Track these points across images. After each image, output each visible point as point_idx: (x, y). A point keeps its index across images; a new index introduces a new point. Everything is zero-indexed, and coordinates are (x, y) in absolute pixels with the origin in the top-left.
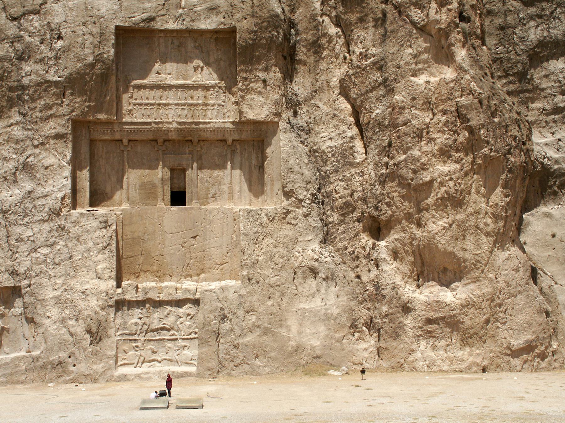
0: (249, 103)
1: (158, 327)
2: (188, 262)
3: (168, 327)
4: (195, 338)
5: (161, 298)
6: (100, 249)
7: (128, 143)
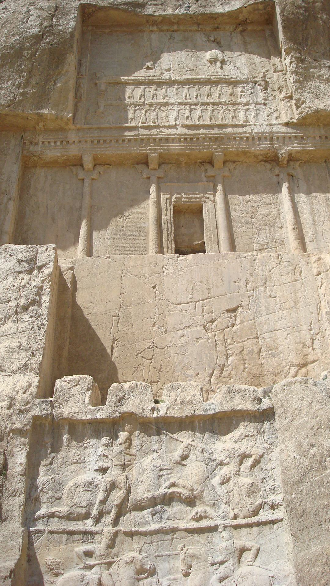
0: (313, 90)
1: (157, 494)
2: (222, 361)
3: (185, 493)
4: (273, 522)
5: (162, 413)
6: (12, 311)
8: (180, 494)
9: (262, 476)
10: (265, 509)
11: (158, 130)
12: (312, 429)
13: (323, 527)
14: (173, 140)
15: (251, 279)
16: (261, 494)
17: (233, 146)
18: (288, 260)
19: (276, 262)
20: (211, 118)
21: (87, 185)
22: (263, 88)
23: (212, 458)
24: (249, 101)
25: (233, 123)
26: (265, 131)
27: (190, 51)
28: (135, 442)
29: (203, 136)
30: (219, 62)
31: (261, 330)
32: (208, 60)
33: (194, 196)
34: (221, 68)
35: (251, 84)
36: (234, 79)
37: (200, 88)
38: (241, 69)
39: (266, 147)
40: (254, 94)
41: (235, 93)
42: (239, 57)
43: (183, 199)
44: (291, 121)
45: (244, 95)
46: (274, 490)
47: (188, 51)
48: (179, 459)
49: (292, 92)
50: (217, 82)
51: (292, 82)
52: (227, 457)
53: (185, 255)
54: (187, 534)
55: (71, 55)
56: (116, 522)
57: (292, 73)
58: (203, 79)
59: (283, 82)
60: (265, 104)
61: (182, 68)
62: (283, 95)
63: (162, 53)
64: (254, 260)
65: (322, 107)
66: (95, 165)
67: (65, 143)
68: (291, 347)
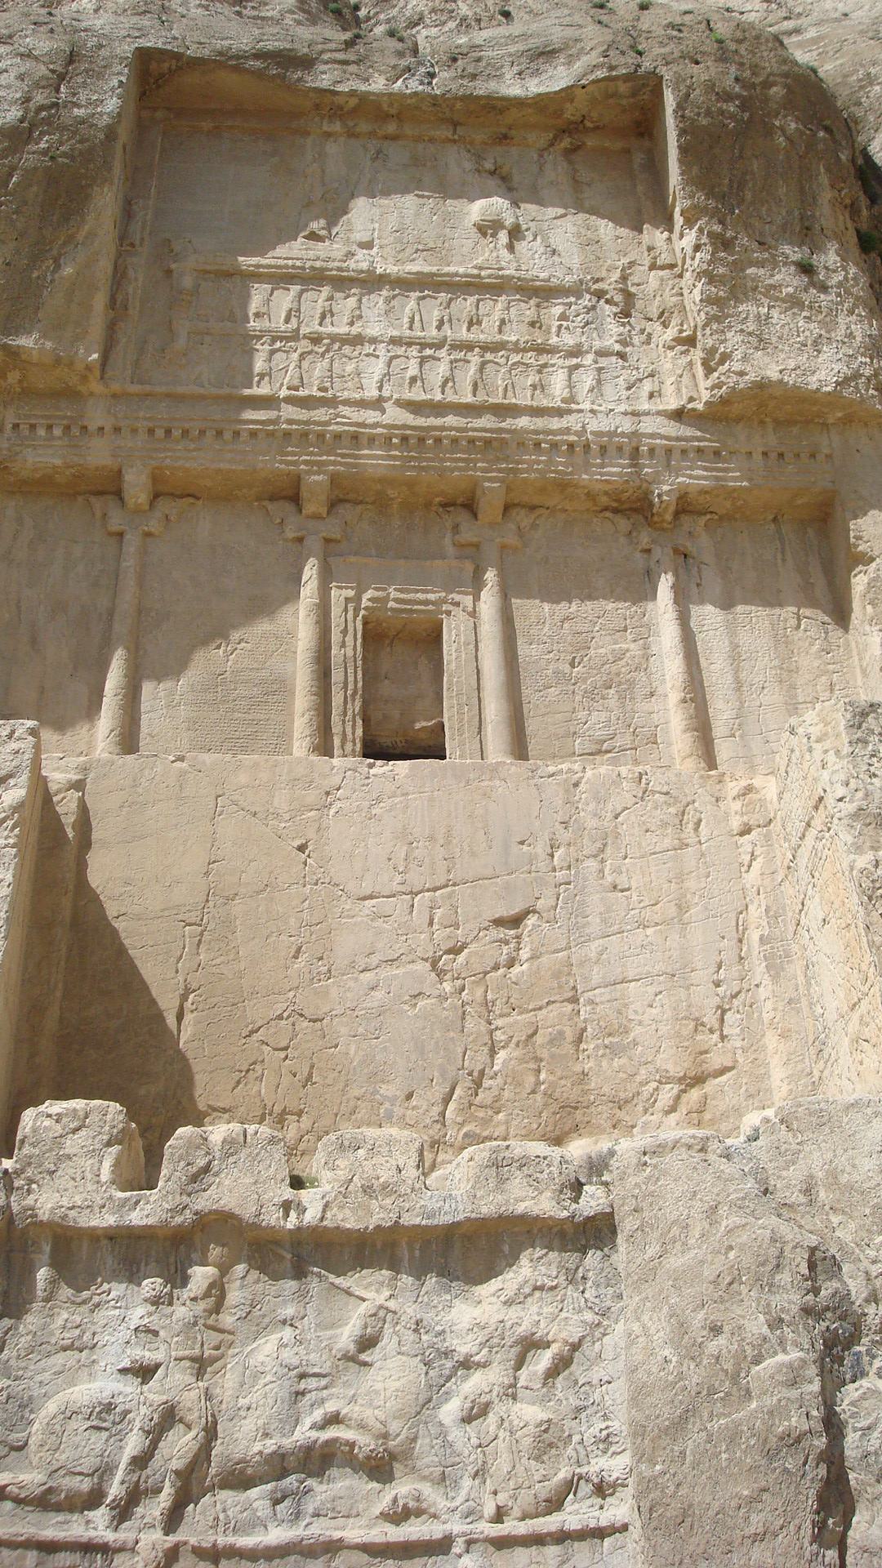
1: (287, 1443)
2: (477, 1059)
3: (365, 1443)
4: (600, 1533)
5: (311, 1216)
7: (152, 504)
8: (352, 1445)
9: (574, 1402)
10: (580, 1494)
11: (332, 411)
12: (715, 1283)
13: (735, 1557)
14: (372, 440)
15: (564, 836)
16: (570, 1451)
17: (531, 467)
18: (665, 789)
19: (634, 793)
20: (475, 386)
21: (132, 549)
22: (618, 310)
23: (443, 1347)
24: (580, 345)
25: (535, 404)
26: (619, 430)
27: (429, 197)
28: (235, 1295)
29: (453, 433)
30: (505, 231)
31: (586, 979)
32: (474, 225)
33: (420, 596)
34: (511, 248)
35: (588, 296)
36: (542, 281)
37: (451, 300)
38: (563, 254)
39: (619, 474)
40: (593, 326)
41: (545, 320)
42: (559, 222)
43: (391, 604)
44: (690, 406)
45: (567, 328)
46: (606, 1441)
47: (422, 197)
48: (352, 1347)
49: (696, 326)
50: (497, 287)
51: (697, 302)
52: (482, 1345)
53: (391, 763)
54: (366, 1558)
55: (106, 189)
56: (173, 1519)
57: (699, 277)
58: (461, 276)
59: (674, 299)
60: (622, 356)
61: (405, 241)
62: (671, 333)
63: (352, 196)
64: (576, 785)
65: (773, 374)
66: (157, 496)
67: (75, 431)
68: (664, 1029)
